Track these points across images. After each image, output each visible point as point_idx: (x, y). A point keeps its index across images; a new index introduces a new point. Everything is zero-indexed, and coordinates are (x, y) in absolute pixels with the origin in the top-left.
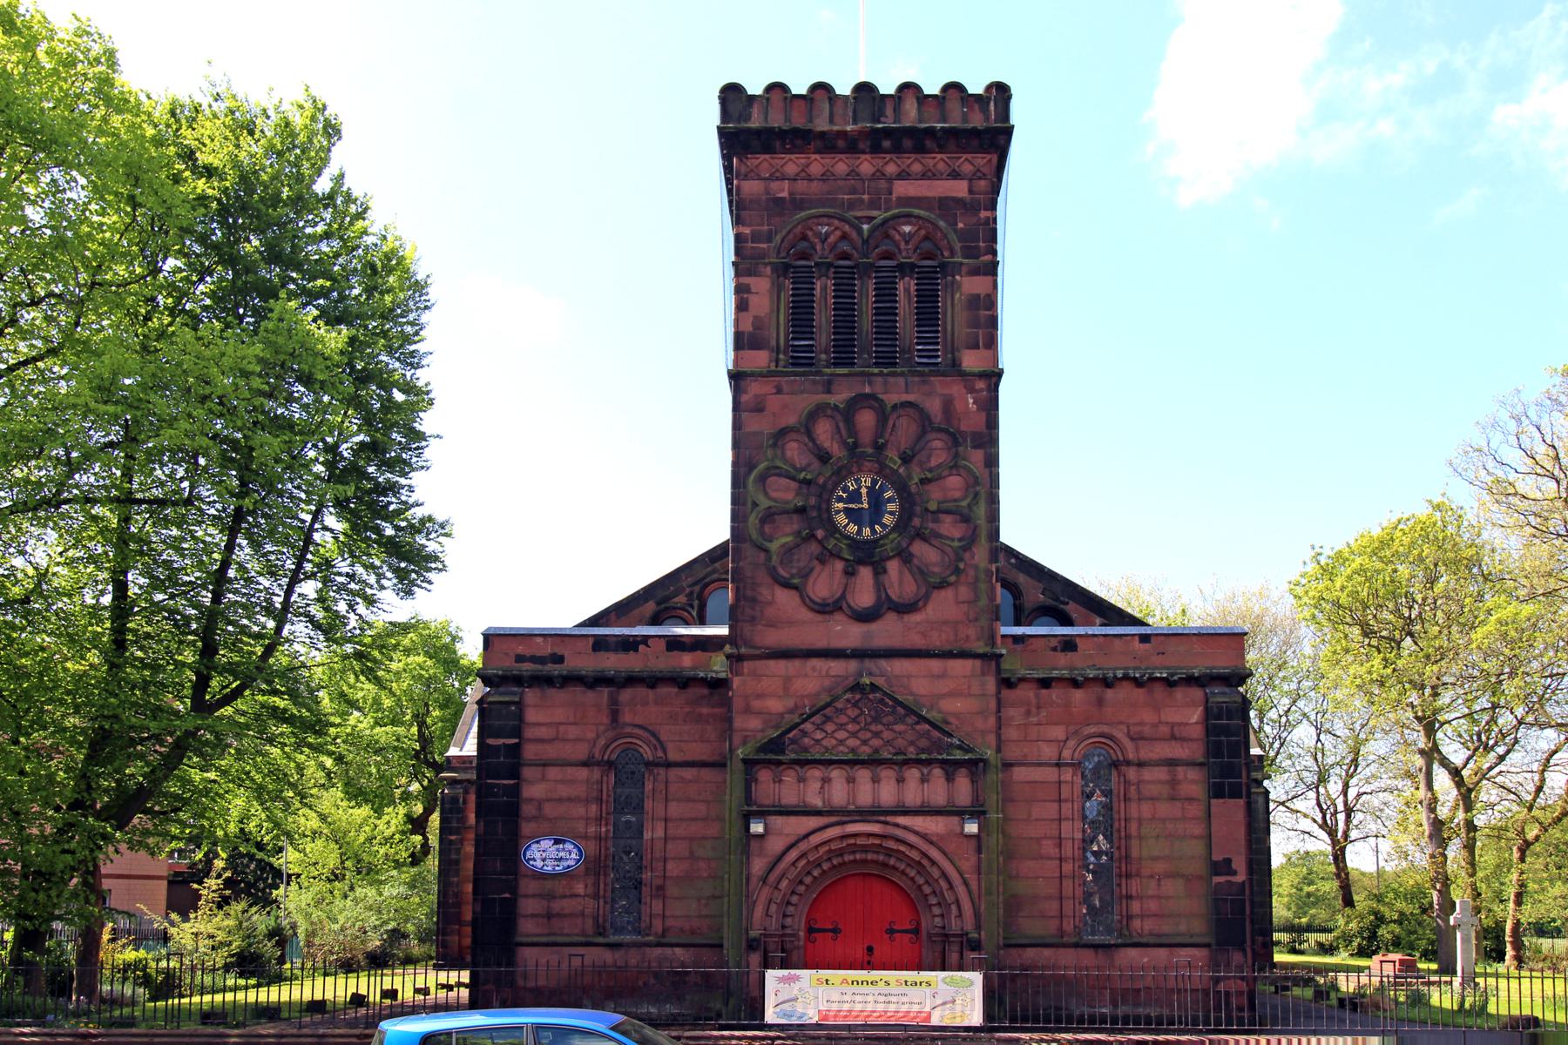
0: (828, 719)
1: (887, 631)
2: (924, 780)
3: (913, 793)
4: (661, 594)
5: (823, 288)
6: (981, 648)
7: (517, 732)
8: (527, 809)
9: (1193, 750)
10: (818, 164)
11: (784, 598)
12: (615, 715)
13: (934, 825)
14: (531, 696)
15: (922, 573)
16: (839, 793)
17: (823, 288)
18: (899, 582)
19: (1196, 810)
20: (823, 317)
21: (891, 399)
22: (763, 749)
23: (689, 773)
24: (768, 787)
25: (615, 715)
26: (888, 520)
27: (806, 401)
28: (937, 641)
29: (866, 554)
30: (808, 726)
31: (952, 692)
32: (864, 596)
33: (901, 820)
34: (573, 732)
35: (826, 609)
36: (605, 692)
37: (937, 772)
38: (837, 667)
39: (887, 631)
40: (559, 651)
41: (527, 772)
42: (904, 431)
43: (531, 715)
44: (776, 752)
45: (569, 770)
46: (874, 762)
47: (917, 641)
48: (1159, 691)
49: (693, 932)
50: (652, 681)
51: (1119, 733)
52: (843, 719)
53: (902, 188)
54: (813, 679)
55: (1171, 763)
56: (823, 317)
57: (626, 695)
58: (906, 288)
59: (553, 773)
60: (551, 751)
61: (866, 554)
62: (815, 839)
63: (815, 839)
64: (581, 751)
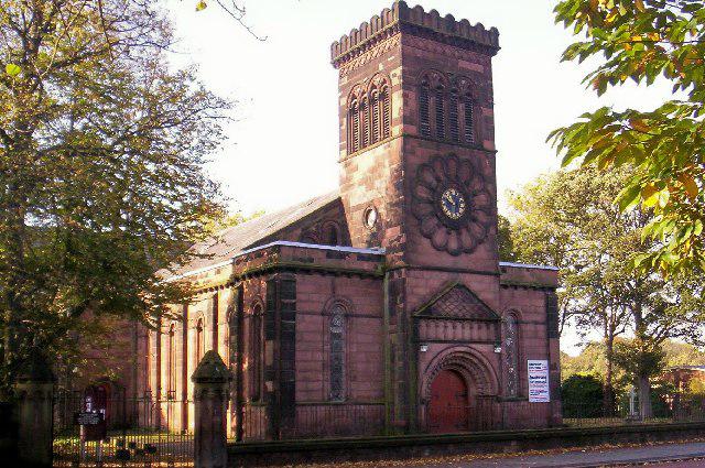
0: (446, 299)
1: (463, 261)
2: (479, 328)
3: (476, 334)
4: (307, 224)
5: (432, 100)
6: (493, 271)
7: (295, 298)
8: (298, 337)
9: (540, 318)
10: (431, 44)
11: (426, 242)
12: (334, 289)
13: (480, 347)
14: (298, 277)
15: (473, 236)
16: (450, 333)
17: (432, 100)
18: (467, 240)
19: (543, 343)
20: (432, 113)
21: (463, 157)
22: (424, 312)
23: (365, 320)
24: (428, 329)
25: (334, 289)
26: (461, 210)
27: (433, 152)
28: (480, 267)
29: (454, 226)
30: (439, 302)
31: (484, 288)
32: (453, 245)
33: (473, 346)
34: (315, 297)
35: (443, 249)
36: (328, 279)
37: (483, 325)
38: (445, 276)
39: (463, 261)
40: (313, 256)
41: (299, 317)
42: (465, 171)
43: (299, 288)
44: (429, 313)
45: (315, 317)
46: (463, 320)
47: (471, 266)
48: (531, 290)
49: (368, 398)
50: (349, 274)
51: (519, 310)
52: (452, 300)
53: (463, 64)
54: (437, 280)
55: (536, 323)
56: (432, 113)
57: (338, 280)
58: (461, 106)
59: (307, 317)
60: (308, 307)
61: (454, 226)
62: (444, 354)
63: (444, 354)
64: (320, 308)
